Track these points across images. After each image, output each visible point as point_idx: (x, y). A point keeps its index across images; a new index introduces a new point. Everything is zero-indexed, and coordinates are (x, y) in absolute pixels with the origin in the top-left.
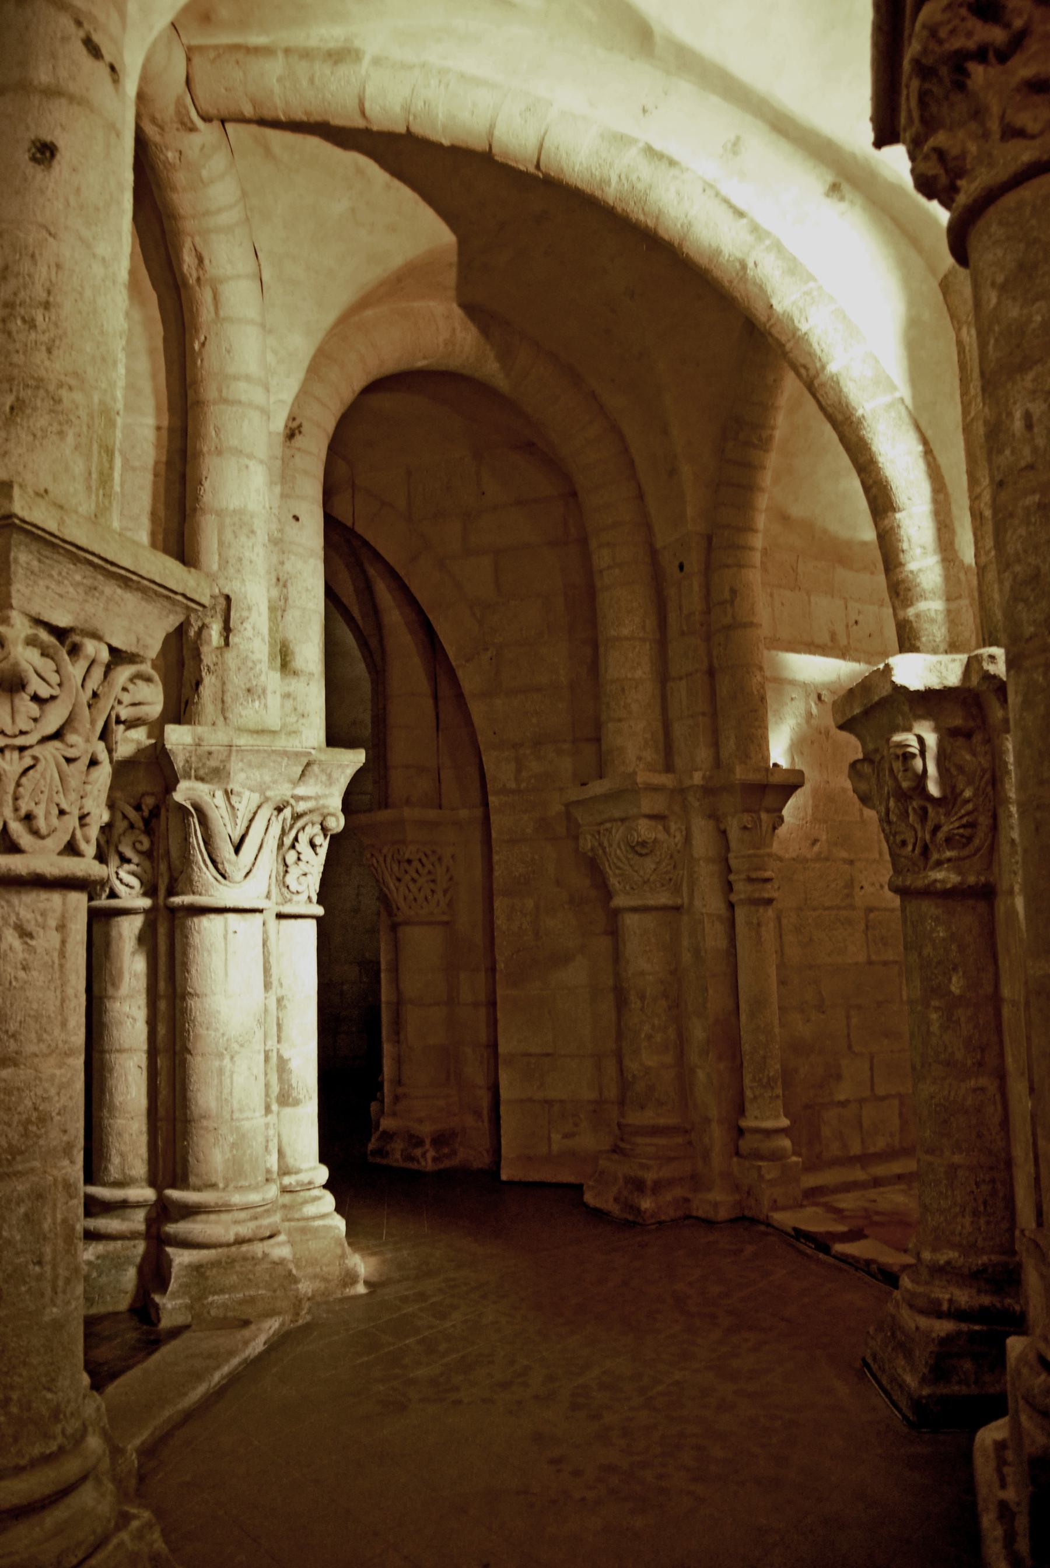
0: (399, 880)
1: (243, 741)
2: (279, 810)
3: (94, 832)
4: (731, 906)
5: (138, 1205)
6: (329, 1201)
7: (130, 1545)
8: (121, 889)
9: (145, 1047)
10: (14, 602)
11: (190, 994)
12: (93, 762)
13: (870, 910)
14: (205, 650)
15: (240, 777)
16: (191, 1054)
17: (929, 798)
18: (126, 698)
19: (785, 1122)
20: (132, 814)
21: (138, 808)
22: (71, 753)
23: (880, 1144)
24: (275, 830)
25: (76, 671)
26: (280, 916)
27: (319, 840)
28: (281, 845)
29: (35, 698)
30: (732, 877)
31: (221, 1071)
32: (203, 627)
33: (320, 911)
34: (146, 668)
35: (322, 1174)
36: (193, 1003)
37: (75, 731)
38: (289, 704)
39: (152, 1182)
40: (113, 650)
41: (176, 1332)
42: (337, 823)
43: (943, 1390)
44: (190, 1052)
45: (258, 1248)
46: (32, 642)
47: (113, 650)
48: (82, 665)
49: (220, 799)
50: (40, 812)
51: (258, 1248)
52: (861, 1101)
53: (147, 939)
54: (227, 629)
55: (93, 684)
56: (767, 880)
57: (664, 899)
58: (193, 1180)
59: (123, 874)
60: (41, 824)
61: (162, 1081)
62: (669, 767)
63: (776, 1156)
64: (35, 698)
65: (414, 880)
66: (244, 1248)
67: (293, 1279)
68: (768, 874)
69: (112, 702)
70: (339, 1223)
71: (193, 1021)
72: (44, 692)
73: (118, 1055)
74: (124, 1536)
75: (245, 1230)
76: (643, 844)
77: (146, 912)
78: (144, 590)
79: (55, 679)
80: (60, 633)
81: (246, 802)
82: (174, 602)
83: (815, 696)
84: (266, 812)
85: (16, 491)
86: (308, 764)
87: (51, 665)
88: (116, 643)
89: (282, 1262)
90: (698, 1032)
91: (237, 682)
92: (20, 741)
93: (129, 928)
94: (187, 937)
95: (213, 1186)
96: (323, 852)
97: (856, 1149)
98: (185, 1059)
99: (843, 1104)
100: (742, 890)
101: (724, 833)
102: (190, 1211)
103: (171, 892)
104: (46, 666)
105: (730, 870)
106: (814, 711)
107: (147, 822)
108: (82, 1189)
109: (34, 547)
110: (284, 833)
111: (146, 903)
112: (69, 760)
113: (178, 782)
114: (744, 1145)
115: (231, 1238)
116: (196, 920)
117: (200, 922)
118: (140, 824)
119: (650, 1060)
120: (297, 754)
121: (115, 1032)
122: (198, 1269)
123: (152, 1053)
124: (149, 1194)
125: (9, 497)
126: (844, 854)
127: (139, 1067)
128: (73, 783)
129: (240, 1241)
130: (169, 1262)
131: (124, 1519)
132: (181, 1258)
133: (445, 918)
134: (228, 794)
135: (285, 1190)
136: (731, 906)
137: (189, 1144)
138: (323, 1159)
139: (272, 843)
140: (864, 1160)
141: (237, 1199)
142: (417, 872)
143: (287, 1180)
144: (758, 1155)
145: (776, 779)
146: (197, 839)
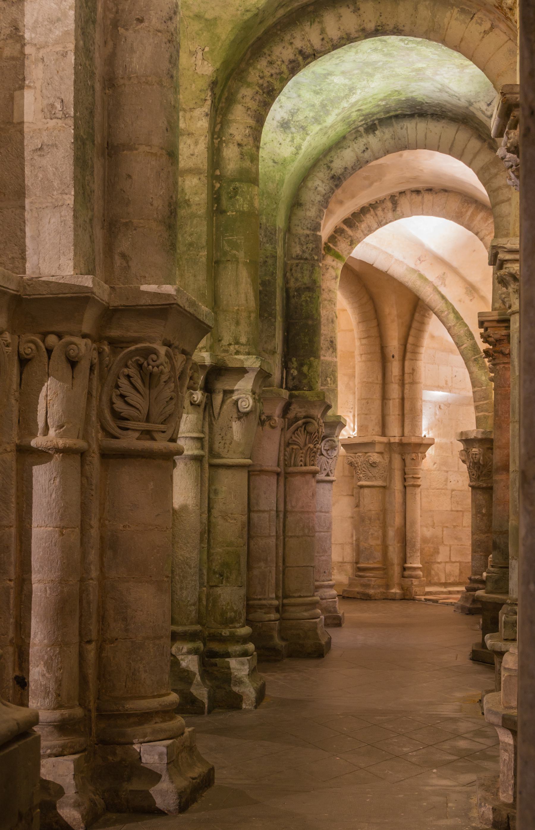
4: (405, 487)
13: (453, 490)
17: (480, 464)
19: (420, 566)
23: (451, 580)
30: (406, 476)
43: (475, 606)
52: (446, 562)
56: (419, 478)
57: (380, 483)
62: (384, 434)
63: (416, 577)
68: (419, 476)
76: (374, 463)
83: (438, 406)
90: (391, 533)
97: (443, 580)
99: (439, 563)
100: (410, 482)
101: (404, 460)
105: (405, 474)
106: (438, 413)
114: (407, 573)
119: (372, 542)
126: (445, 469)
140: (445, 585)
144: (411, 577)
145: (424, 442)
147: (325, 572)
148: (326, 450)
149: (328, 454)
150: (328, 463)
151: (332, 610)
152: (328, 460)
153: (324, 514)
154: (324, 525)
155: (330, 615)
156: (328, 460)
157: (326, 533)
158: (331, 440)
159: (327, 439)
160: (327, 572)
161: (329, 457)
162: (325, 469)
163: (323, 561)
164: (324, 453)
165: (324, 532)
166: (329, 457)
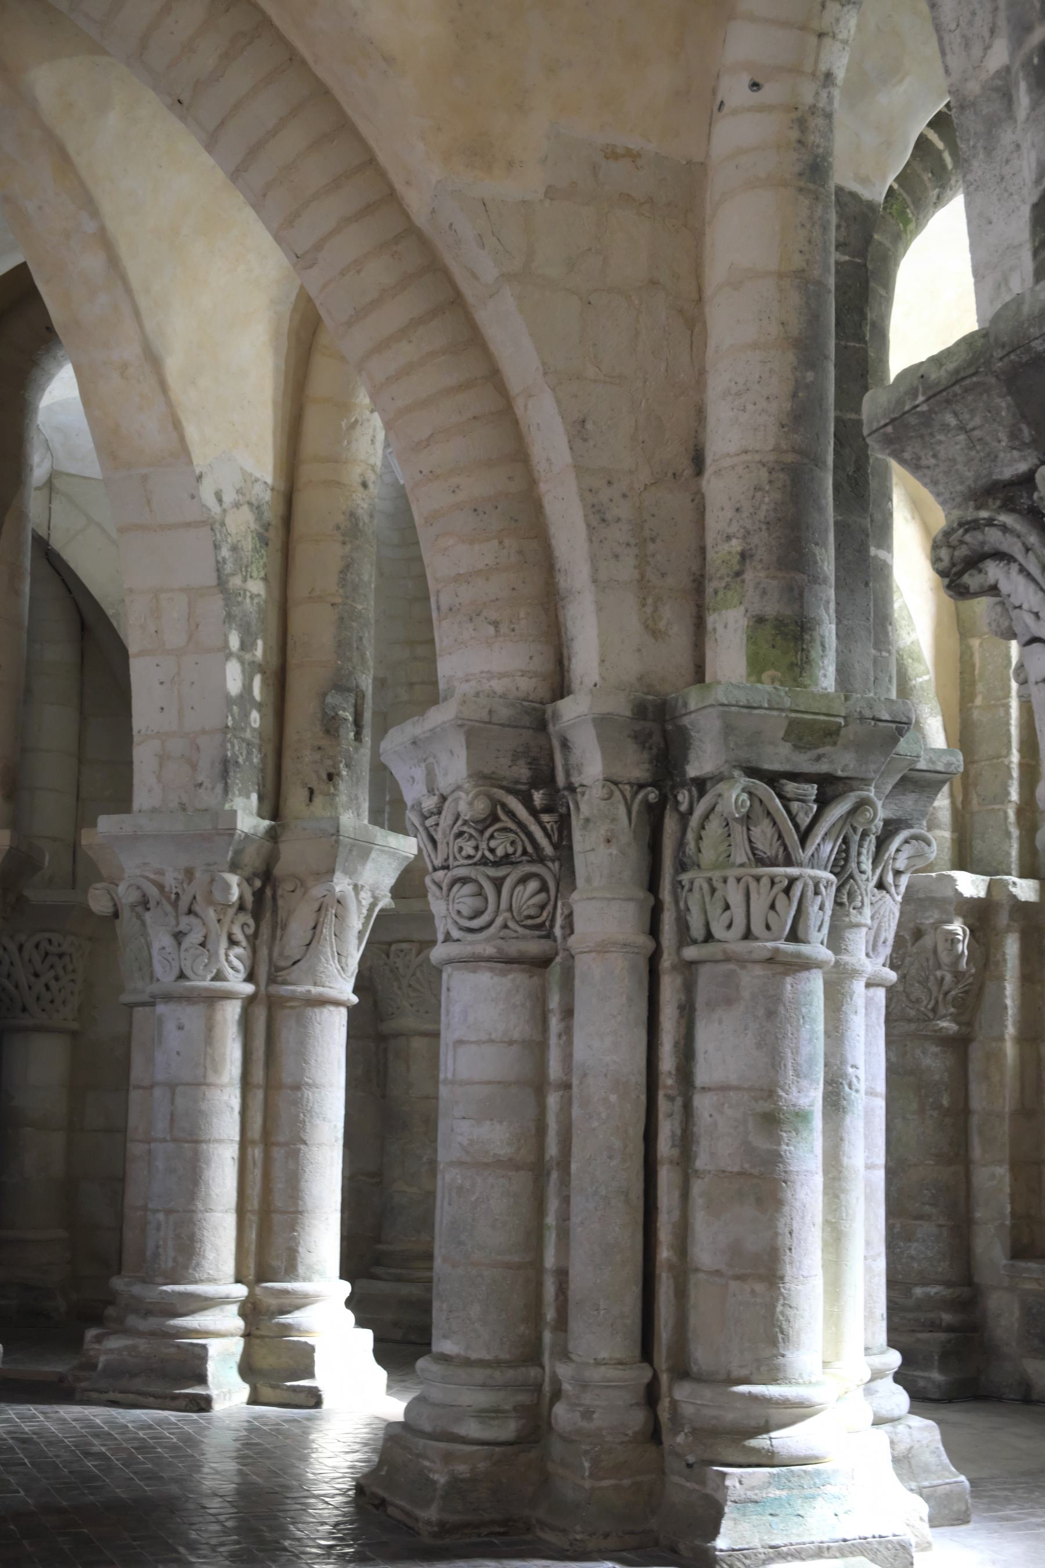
0: (36, 975)
8: (229, 972)
9: (237, 1138)
11: (307, 1084)
16: (306, 1144)
44: (305, 1143)
59: (232, 958)
61: (256, 1174)
65: (57, 978)
71: (309, 1111)
73: (216, 1145)
94: (305, 1027)
98: (299, 1150)
103: (272, 980)
116: (317, 1010)
117: (321, 1013)
121: (215, 1120)
123: (244, 1144)
127: (233, 1158)
133: (75, 1026)
137: (299, 1235)
142: (64, 968)
158: (916, 838)
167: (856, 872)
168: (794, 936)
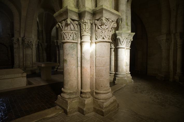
1: (123, 32)
2: (126, 39)
3: (111, 37)
5: (113, 73)
6: (130, 75)
7: (113, 98)
8: (112, 46)
10: (103, 16)
12: (111, 31)
14: (119, 24)
15: (123, 36)
18: (113, 25)
20: (113, 39)
21: (113, 39)
22: (109, 30)
24: (126, 40)
25: (109, 22)
26: (126, 49)
27: (130, 42)
28: (127, 42)
29: (106, 25)
31: (121, 62)
32: (119, 21)
33: (130, 48)
34: (115, 22)
35: (130, 72)
36: (118, 56)
37: (109, 28)
38: (128, 29)
39: (115, 72)
40: (112, 21)
41: (116, 84)
42: (132, 40)
45: (124, 78)
46: (105, 20)
47: (112, 21)
48: (110, 22)
49: (121, 38)
50: (106, 36)
51: (124, 78)
53: (114, 51)
54: (122, 22)
55: (110, 24)
58: (118, 72)
60: (106, 36)
64: (106, 25)
66: (123, 78)
67: (127, 81)
69: (112, 26)
70: (131, 77)
72: (106, 25)
74: (113, 97)
75: (123, 76)
77: (114, 48)
78: (115, 15)
79: (107, 23)
80: (107, 19)
81: (123, 38)
82: (118, 16)
84: (125, 39)
85: (103, 6)
86: (129, 34)
87: (107, 22)
88: (112, 20)
89: (126, 79)
91: (122, 27)
92: (104, 29)
93: (113, 50)
95: (120, 72)
96: (131, 43)
101: (177, 41)
102: (118, 74)
104: (106, 22)
107: (114, 40)
108: (110, 72)
109: (105, 10)
110: (127, 41)
111: (114, 47)
112: (109, 31)
113: (117, 36)
115: (121, 77)
118: (113, 40)
120: (128, 33)
122: (118, 79)
124: (114, 73)
125: (103, 6)
128: (109, 33)
129: (122, 77)
130: (116, 78)
131: (113, 96)
132: (117, 78)
134: (122, 37)
135: (126, 73)
136: (177, 49)
138: (130, 71)
139: (126, 42)
141: (122, 74)
143: (126, 73)
146: (119, 42)
147: (102, 86)
148: (100, 26)
149: (101, 27)
150: (102, 32)
151: (102, 106)
152: (102, 31)
153: (101, 58)
154: (101, 63)
155: (100, 109)
156: (102, 31)
157: (102, 68)
159: (100, 20)
160: (103, 86)
161: (103, 29)
162: (101, 36)
163: (101, 81)
164: (100, 27)
165: (102, 67)
166: (103, 29)
167: (82, 29)
168: (64, 40)
